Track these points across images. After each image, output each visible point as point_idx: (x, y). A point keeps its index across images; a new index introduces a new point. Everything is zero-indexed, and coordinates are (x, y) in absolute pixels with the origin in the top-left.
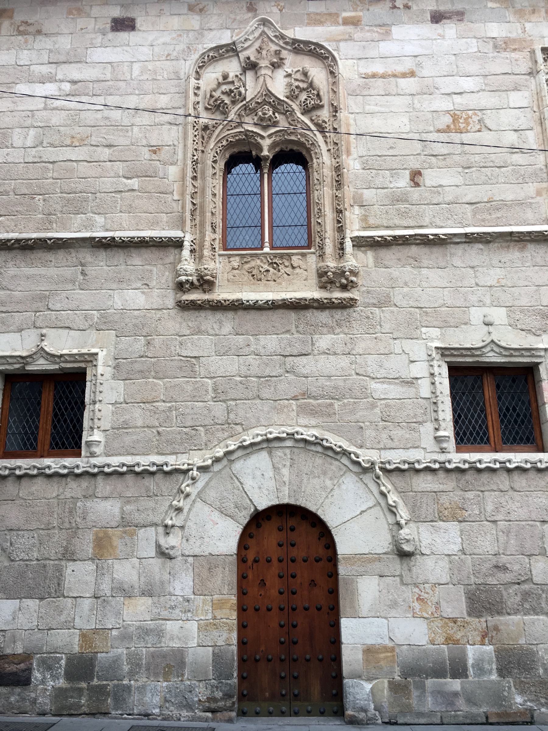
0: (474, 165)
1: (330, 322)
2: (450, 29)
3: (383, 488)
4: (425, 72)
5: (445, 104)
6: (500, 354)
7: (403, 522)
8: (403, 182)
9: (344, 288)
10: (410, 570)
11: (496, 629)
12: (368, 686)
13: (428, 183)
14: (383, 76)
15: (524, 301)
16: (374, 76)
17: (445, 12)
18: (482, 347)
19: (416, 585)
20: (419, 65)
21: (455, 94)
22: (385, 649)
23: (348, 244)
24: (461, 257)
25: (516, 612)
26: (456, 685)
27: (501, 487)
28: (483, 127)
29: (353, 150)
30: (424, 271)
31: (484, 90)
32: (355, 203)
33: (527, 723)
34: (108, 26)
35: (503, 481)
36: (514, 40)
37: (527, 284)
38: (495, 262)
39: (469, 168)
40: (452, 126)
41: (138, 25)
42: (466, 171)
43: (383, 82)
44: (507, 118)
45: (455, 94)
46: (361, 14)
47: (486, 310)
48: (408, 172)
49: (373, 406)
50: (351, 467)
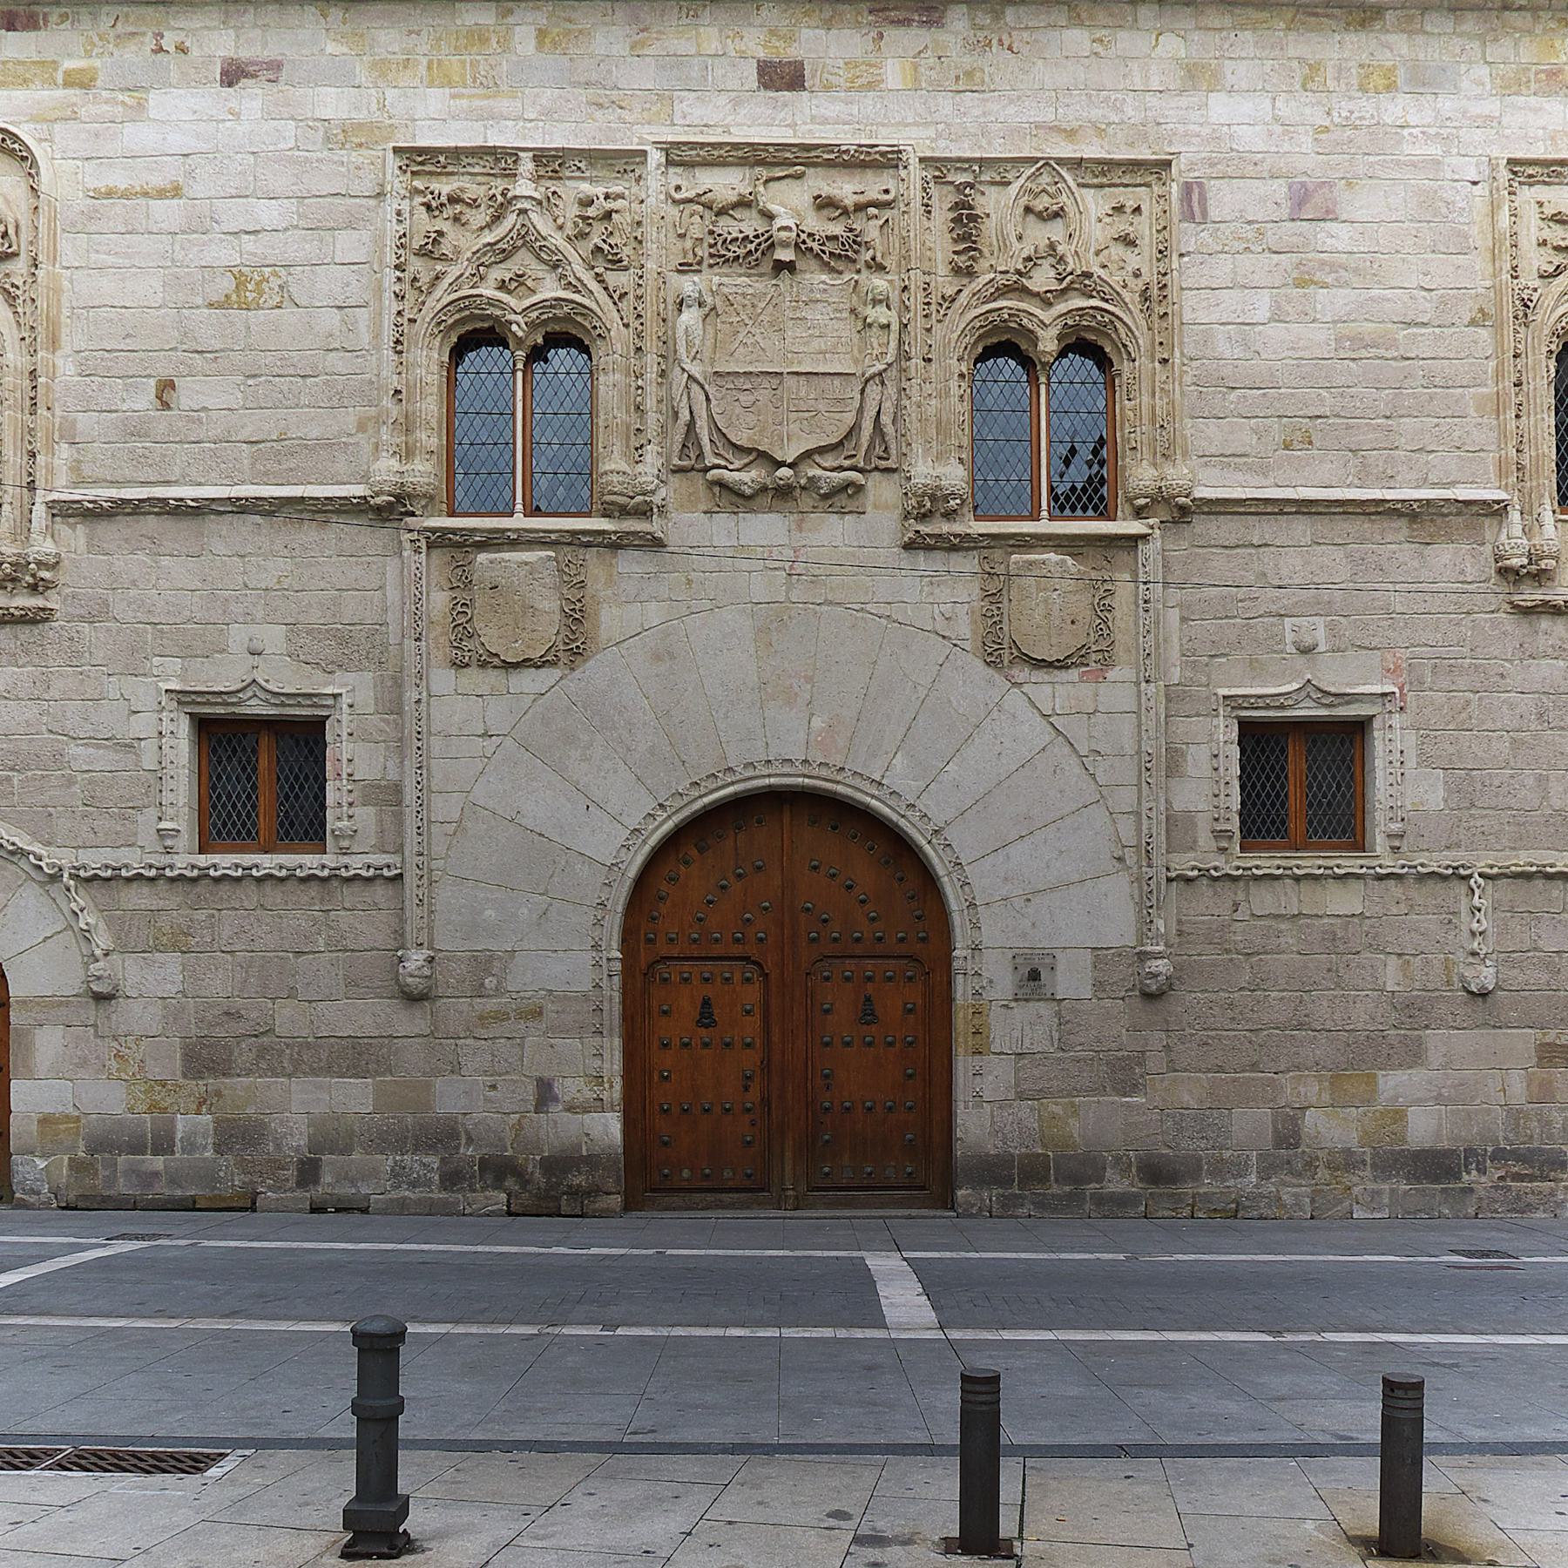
0: (264, 370)
1: (12, 645)
2: (251, 98)
3: (73, 905)
4: (198, 189)
5: (224, 254)
6: (266, 701)
7: (98, 952)
8: (144, 400)
9: (33, 588)
10: (108, 1018)
11: (219, 1094)
12: (41, 1164)
13: (185, 402)
14: (126, 195)
15: (315, 616)
16: (110, 194)
18: (238, 691)
19: (115, 1038)
20: (190, 174)
21: (247, 233)
22: (68, 1118)
23: (40, 511)
24: (224, 536)
25: (249, 1073)
26: (158, 1163)
27: (246, 904)
28: (286, 299)
29: (64, 338)
30: (165, 561)
31: (296, 227)
32: (61, 437)
33: (246, 1209)
35: (250, 896)
37: (322, 585)
38: (278, 546)
39: (255, 376)
40: (234, 297)
42: (250, 382)
43: (125, 206)
44: (329, 284)
45: (247, 233)
46: (97, 63)
47: (254, 629)
48: (152, 382)
49: (70, 782)
50: (33, 874)
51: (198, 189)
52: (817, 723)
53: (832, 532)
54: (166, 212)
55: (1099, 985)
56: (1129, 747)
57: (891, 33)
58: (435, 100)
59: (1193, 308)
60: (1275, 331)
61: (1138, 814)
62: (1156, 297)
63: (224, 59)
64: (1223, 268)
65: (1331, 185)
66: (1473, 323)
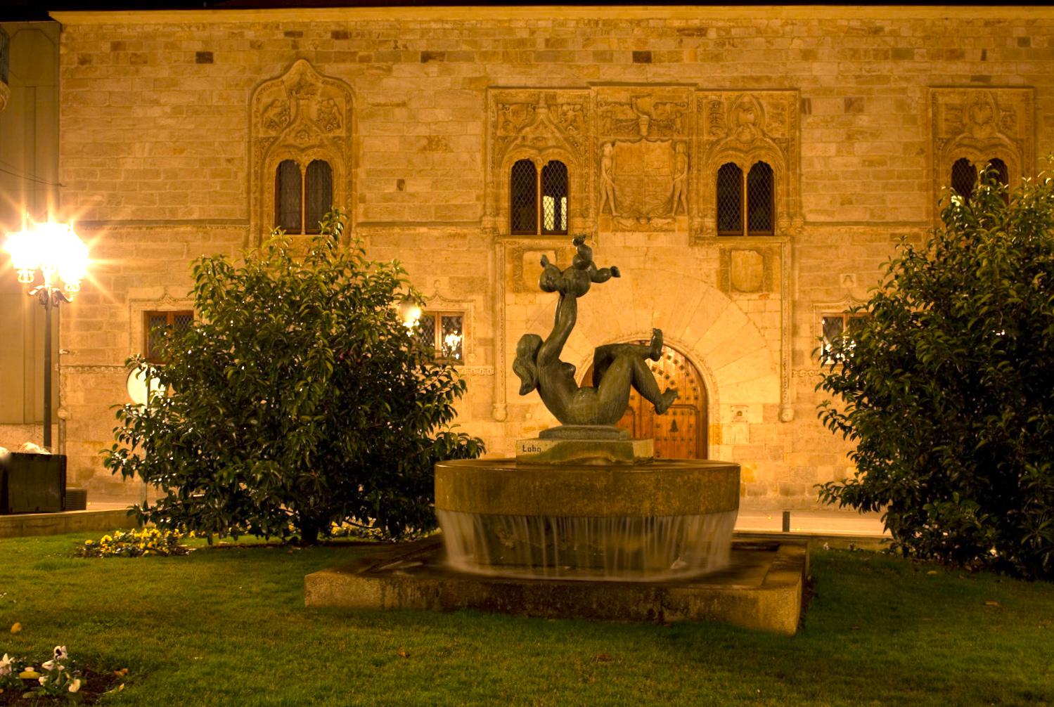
2: (433, 67)
5: (423, 131)
8: (392, 189)
14: (385, 105)
16: (378, 105)
17: (432, 53)
28: (447, 149)
34: (194, 59)
36: (476, 79)
41: (215, 59)
51: (414, 105)
52: (656, 315)
53: (662, 240)
54: (399, 113)
55: (765, 418)
56: (779, 325)
57: (686, 40)
58: (505, 68)
59: (806, 152)
60: (839, 160)
61: (781, 351)
62: (790, 147)
63: (422, 52)
64: (818, 133)
65: (861, 99)
66: (918, 154)
